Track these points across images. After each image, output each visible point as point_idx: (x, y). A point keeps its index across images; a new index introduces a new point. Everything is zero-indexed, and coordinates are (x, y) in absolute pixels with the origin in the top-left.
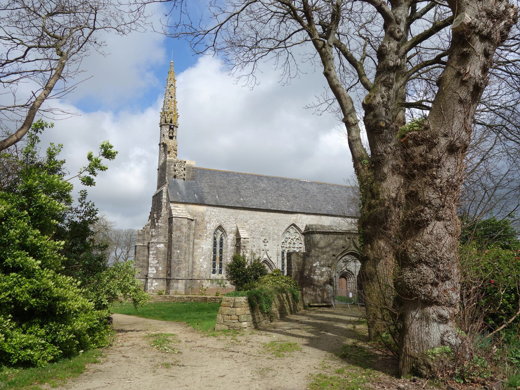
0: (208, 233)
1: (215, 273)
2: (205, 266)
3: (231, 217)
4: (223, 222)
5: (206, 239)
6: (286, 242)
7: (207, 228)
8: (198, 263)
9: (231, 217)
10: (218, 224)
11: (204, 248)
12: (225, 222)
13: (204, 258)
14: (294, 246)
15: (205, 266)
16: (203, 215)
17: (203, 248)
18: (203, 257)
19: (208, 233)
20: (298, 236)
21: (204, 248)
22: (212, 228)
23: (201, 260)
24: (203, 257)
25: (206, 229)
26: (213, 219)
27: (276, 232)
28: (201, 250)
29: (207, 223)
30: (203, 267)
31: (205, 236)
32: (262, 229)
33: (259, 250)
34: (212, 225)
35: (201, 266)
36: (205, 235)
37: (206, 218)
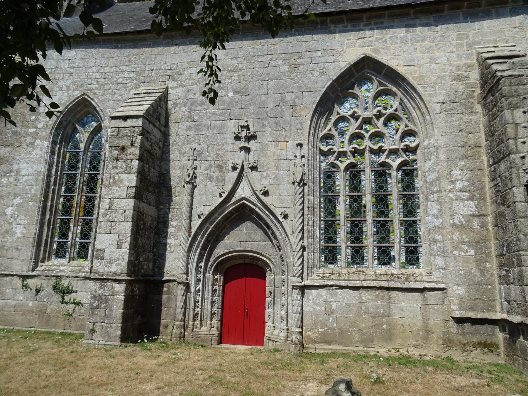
1: (63, 257)
2: (19, 231)
3: (124, 68)
4: (94, 86)
5: (32, 144)
6: (342, 133)
9: (124, 68)
10: (77, 94)
11: (23, 173)
12: (103, 85)
14: (376, 147)
15: (19, 231)
17: (18, 171)
18: (18, 201)
19: (40, 126)
20: (396, 104)
21: (23, 173)
23: (9, 211)
24: (18, 201)
27: (289, 97)
28: (12, 179)
30: (13, 234)
32: (231, 94)
33: (220, 167)
35: (7, 232)
36: (32, 130)
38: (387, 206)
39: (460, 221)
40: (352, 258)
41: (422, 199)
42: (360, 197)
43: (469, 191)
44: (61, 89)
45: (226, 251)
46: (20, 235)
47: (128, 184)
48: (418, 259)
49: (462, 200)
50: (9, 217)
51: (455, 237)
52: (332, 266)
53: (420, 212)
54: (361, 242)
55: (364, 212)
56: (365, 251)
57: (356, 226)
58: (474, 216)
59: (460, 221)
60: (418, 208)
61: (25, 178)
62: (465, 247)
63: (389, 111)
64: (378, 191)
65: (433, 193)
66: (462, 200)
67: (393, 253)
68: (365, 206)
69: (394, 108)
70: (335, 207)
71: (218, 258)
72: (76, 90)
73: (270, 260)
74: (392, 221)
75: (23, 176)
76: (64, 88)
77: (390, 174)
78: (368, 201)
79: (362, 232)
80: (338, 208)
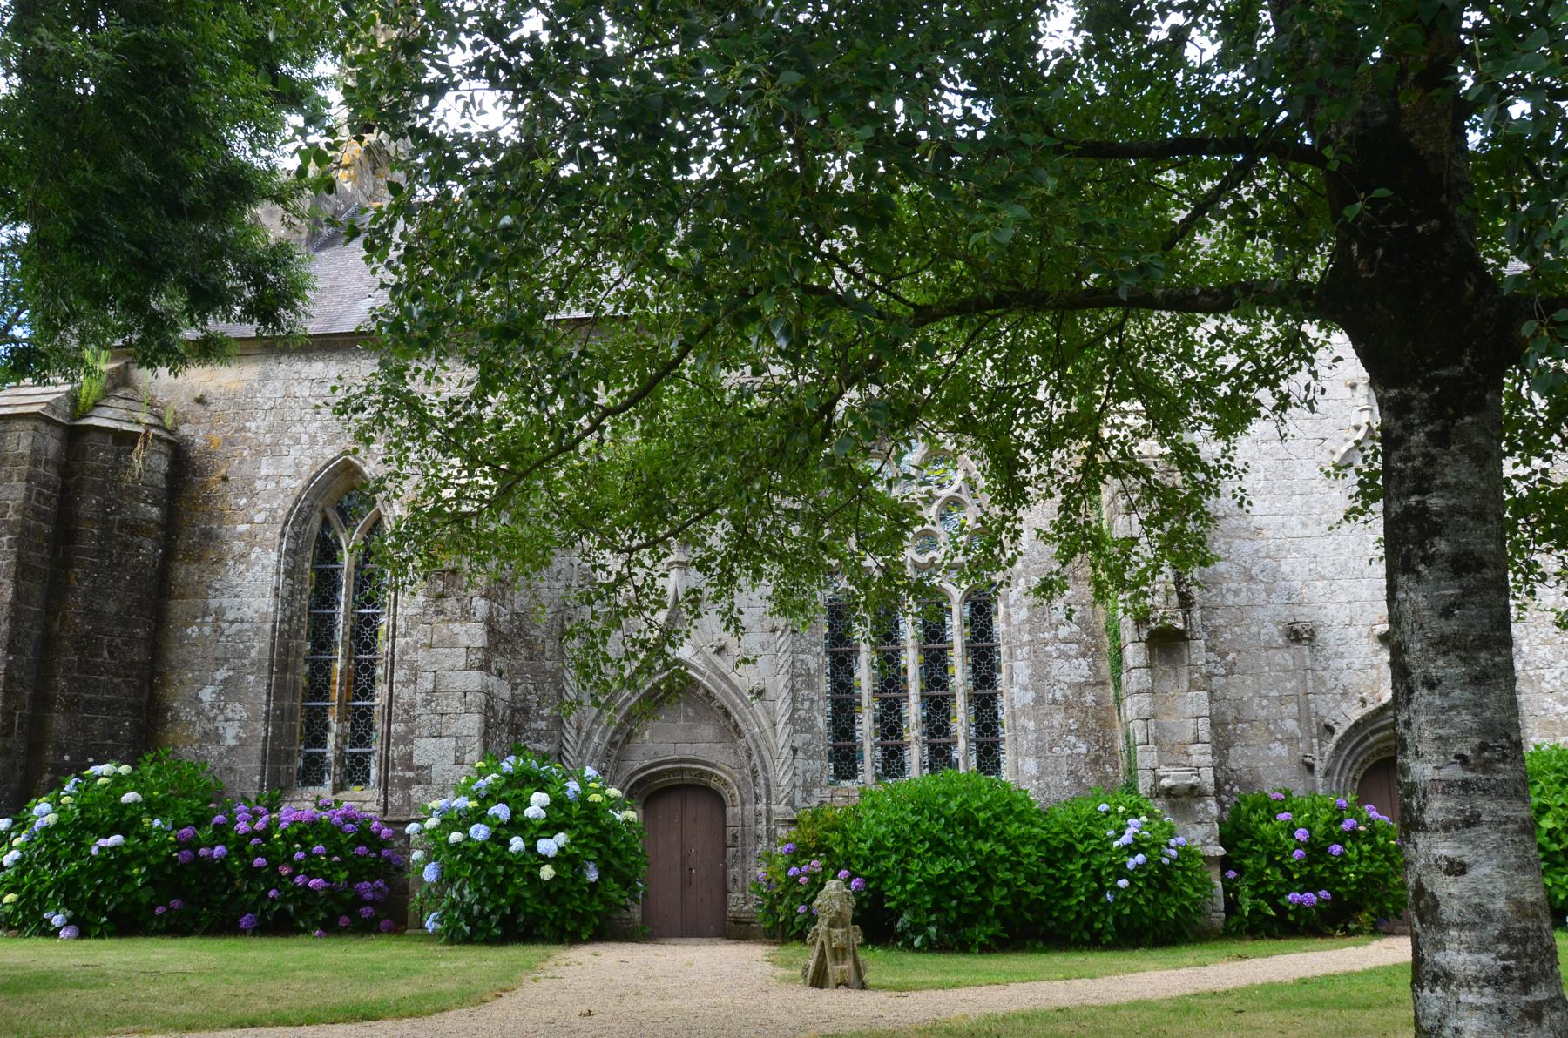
0: (259, 518)
2: (230, 734)
7: (259, 485)
8: (187, 713)
10: (331, 452)
11: (230, 615)
13: (225, 680)
16: (241, 405)
17: (220, 612)
18: (222, 674)
19: (259, 518)
21: (230, 615)
22: (286, 482)
23: (207, 694)
24: (222, 674)
25: (253, 494)
26: (298, 428)
28: (207, 630)
29: (258, 453)
30: (218, 738)
31: (240, 536)
34: (289, 460)
37: (257, 427)
38: (946, 671)
39: (1066, 696)
40: (884, 767)
41: (1004, 657)
42: (897, 652)
43: (1078, 642)
44: (297, 441)
45: (647, 762)
46: (233, 743)
47: (468, 643)
48: (998, 763)
49: (1068, 657)
50: (207, 707)
51: (1056, 723)
52: (847, 783)
53: (1002, 678)
54: (899, 737)
55: (905, 681)
56: (906, 753)
57: (891, 707)
58: (1087, 684)
59: (1066, 696)
60: (999, 671)
61: (237, 626)
62: (1072, 739)
63: (948, 492)
64: (928, 641)
65: (1022, 646)
66: (1068, 657)
67: (955, 755)
68: (905, 671)
69: (954, 488)
70: (851, 674)
71: (632, 775)
72: (331, 442)
73: (731, 776)
74: (953, 696)
75: (232, 622)
76: (305, 438)
77: (949, 611)
78: (911, 660)
79: (901, 719)
80: (857, 675)
